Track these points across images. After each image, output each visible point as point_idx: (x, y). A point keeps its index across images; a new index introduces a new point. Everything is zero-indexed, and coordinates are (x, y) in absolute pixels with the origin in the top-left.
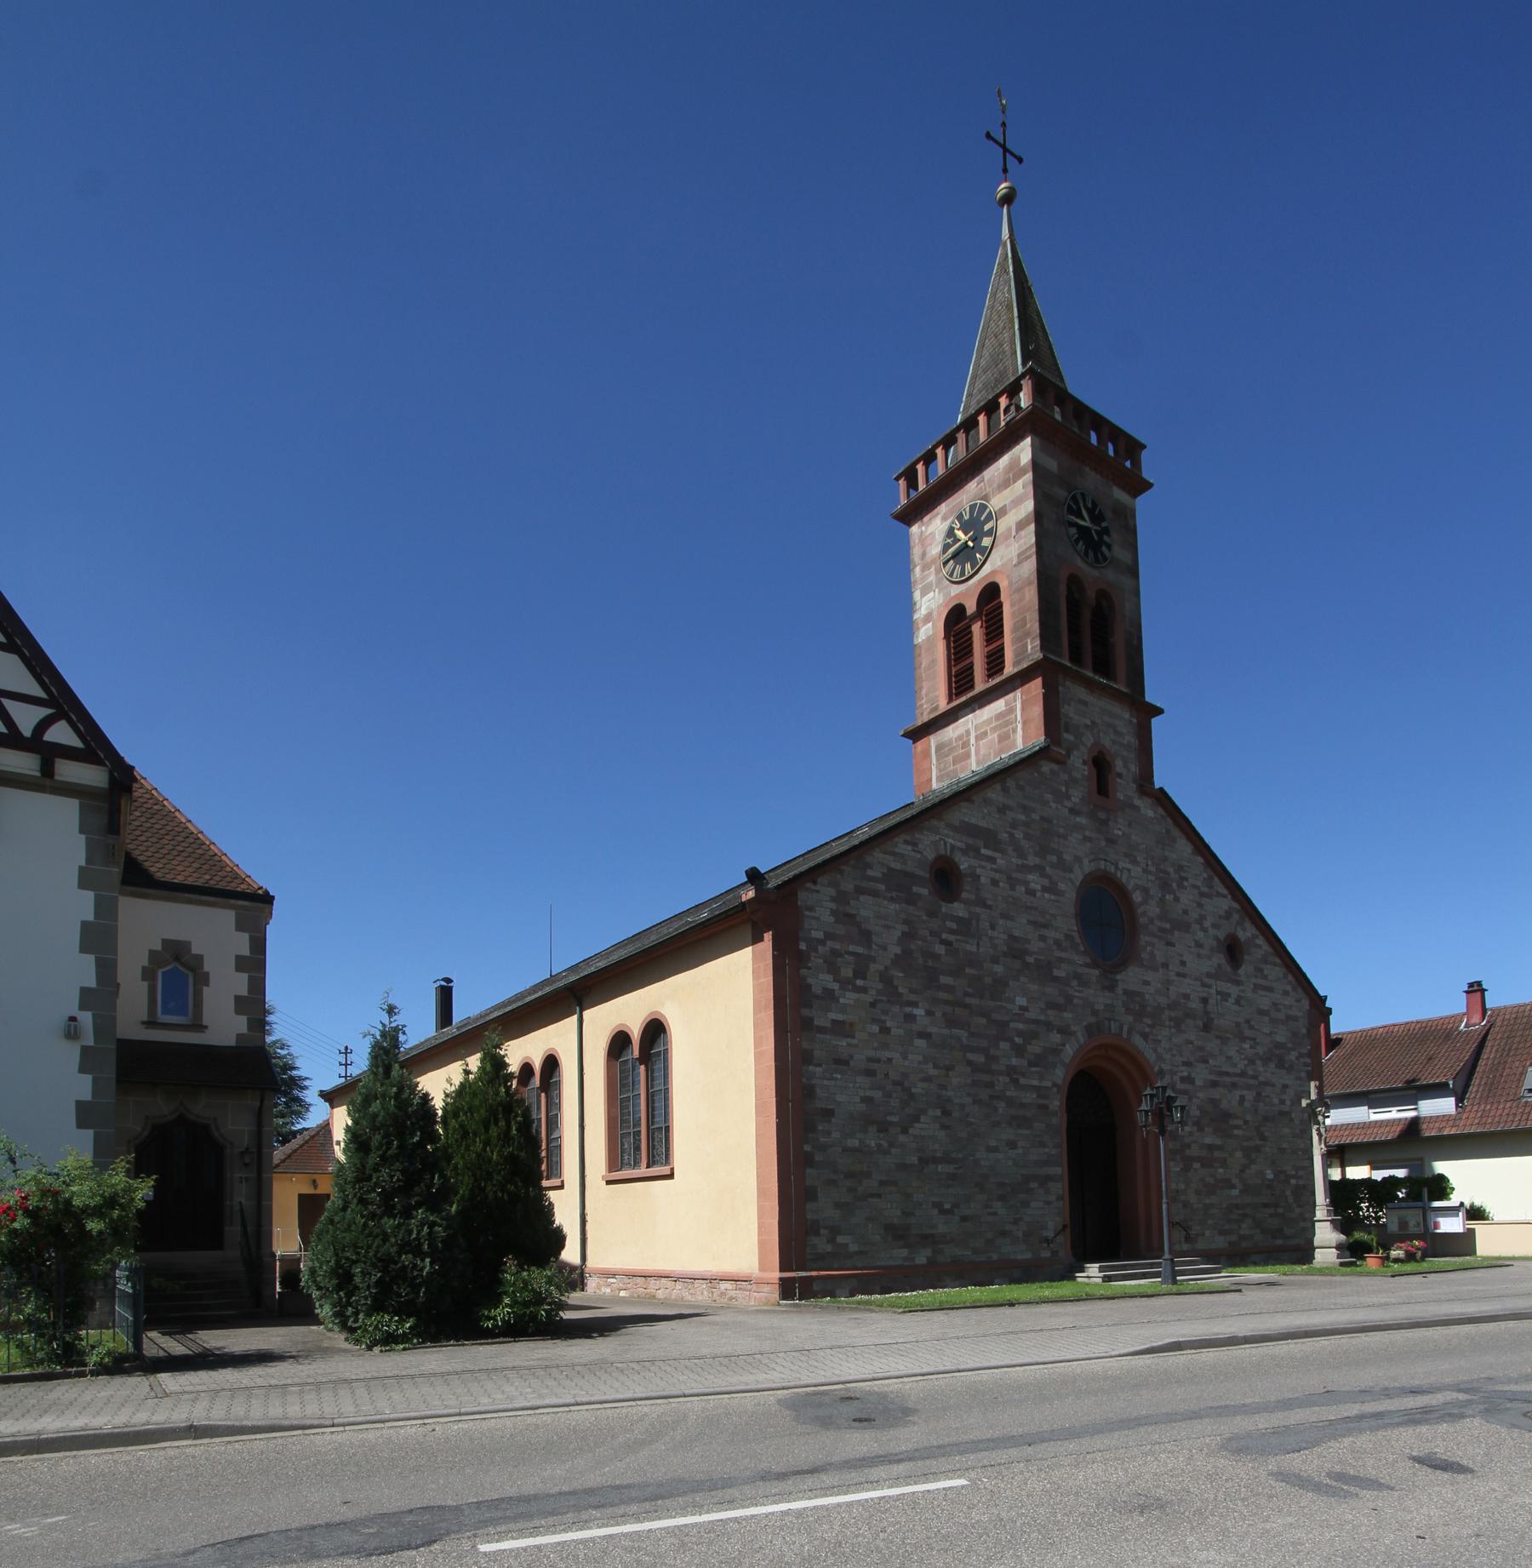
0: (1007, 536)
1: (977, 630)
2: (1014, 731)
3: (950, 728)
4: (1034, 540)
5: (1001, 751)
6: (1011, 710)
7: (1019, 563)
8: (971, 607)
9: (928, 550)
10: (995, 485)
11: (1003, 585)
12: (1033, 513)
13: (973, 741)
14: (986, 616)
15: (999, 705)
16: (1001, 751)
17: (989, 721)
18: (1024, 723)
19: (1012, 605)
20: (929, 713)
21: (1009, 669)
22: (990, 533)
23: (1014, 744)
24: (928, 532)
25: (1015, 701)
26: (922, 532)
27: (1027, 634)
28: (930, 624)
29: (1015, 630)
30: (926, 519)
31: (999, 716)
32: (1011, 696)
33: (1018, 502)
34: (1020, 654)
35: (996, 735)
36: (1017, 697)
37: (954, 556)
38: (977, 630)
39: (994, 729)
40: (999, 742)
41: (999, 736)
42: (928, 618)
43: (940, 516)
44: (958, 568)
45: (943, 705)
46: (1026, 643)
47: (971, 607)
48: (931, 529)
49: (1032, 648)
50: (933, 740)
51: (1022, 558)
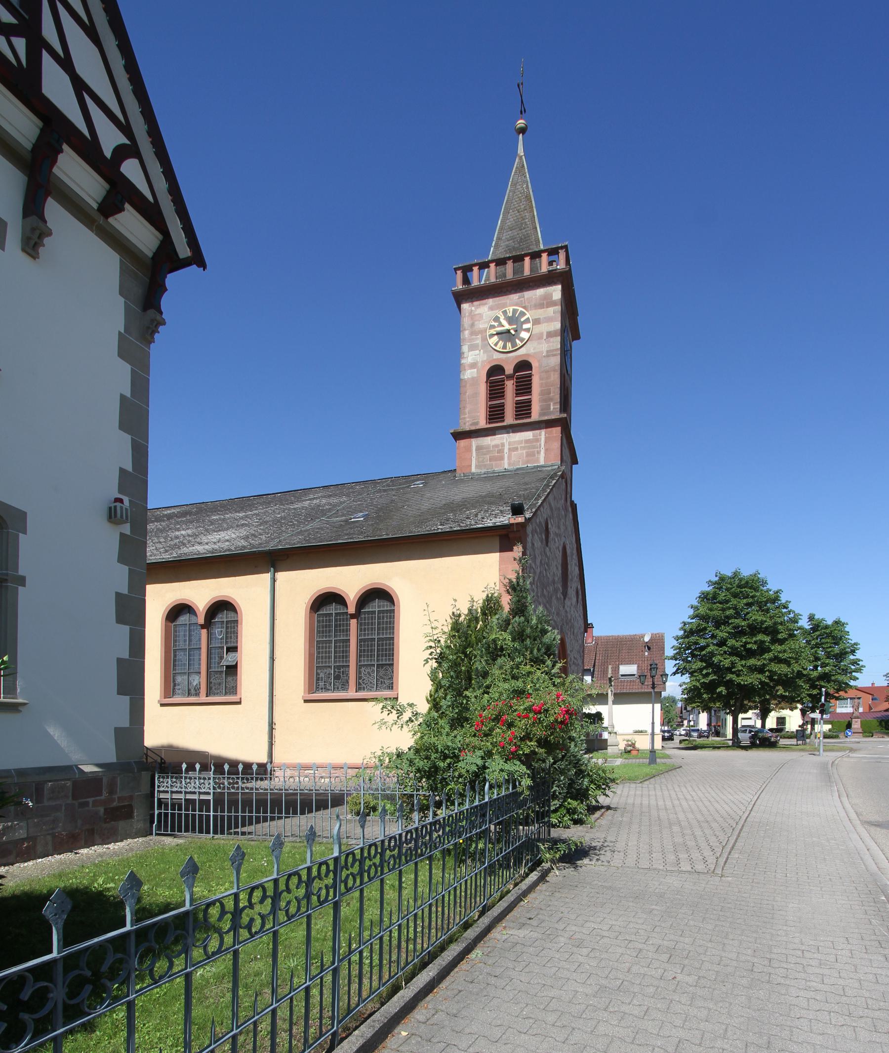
0: (540, 337)
1: (510, 386)
2: (539, 452)
3: (489, 438)
4: (559, 346)
5: (528, 462)
6: (538, 440)
7: (548, 356)
8: (509, 369)
9: (476, 323)
10: (533, 303)
11: (535, 365)
12: (559, 331)
13: (506, 450)
14: (517, 379)
15: (529, 435)
16: (528, 462)
17: (520, 442)
18: (546, 450)
19: (541, 379)
20: (471, 425)
21: (535, 416)
22: (527, 330)
23: (538, 460)
24: (477, 313)
25: (540, 435)
26: (472, 311)
27: (551, 399)
28: (476, 370)
29: (542, 393)
30: (476, 303)
31: (527, 441)
32: (538, 432)
33: (549, 320)
34: (545, 410)
35: (524, 451)
36: (543, 434)
37: (498, 334)
38: (510, 386)
39: (523, 448)
40: (527, 456)
41: (526, 452)
42: (473, 365)
43: (487, 306)
44: (501, 344)
45: (482, 423)
46: (550, 405)
47: (509, 369)
48: (479, 311)
49: (554, 409)
50: (475, 442)
51: (550, 354)
